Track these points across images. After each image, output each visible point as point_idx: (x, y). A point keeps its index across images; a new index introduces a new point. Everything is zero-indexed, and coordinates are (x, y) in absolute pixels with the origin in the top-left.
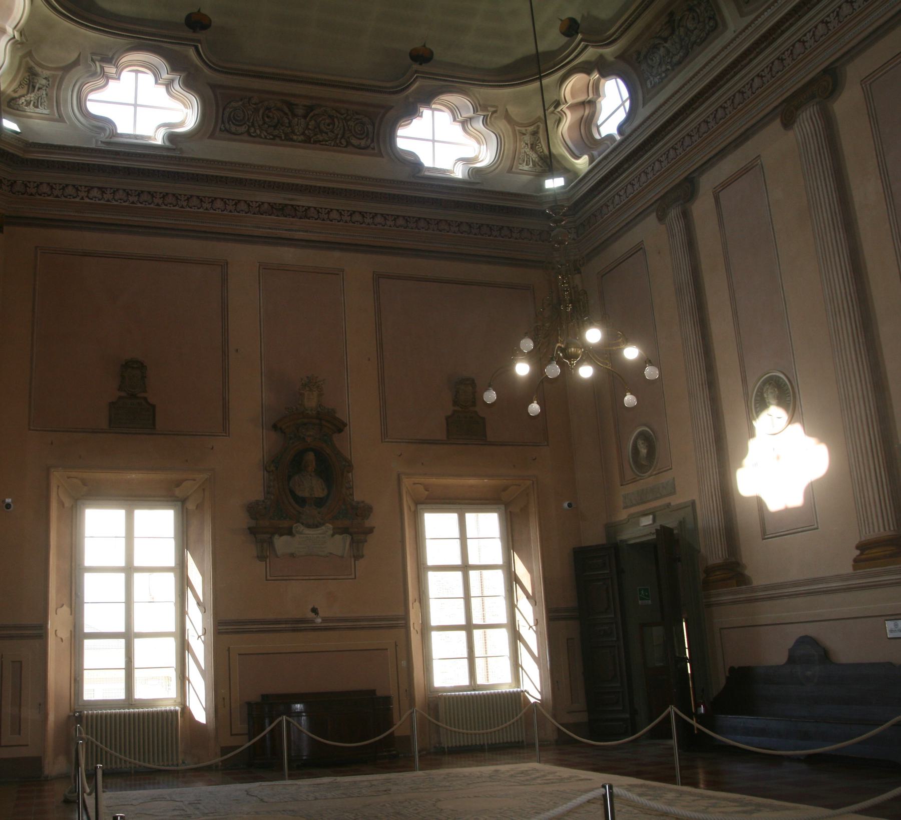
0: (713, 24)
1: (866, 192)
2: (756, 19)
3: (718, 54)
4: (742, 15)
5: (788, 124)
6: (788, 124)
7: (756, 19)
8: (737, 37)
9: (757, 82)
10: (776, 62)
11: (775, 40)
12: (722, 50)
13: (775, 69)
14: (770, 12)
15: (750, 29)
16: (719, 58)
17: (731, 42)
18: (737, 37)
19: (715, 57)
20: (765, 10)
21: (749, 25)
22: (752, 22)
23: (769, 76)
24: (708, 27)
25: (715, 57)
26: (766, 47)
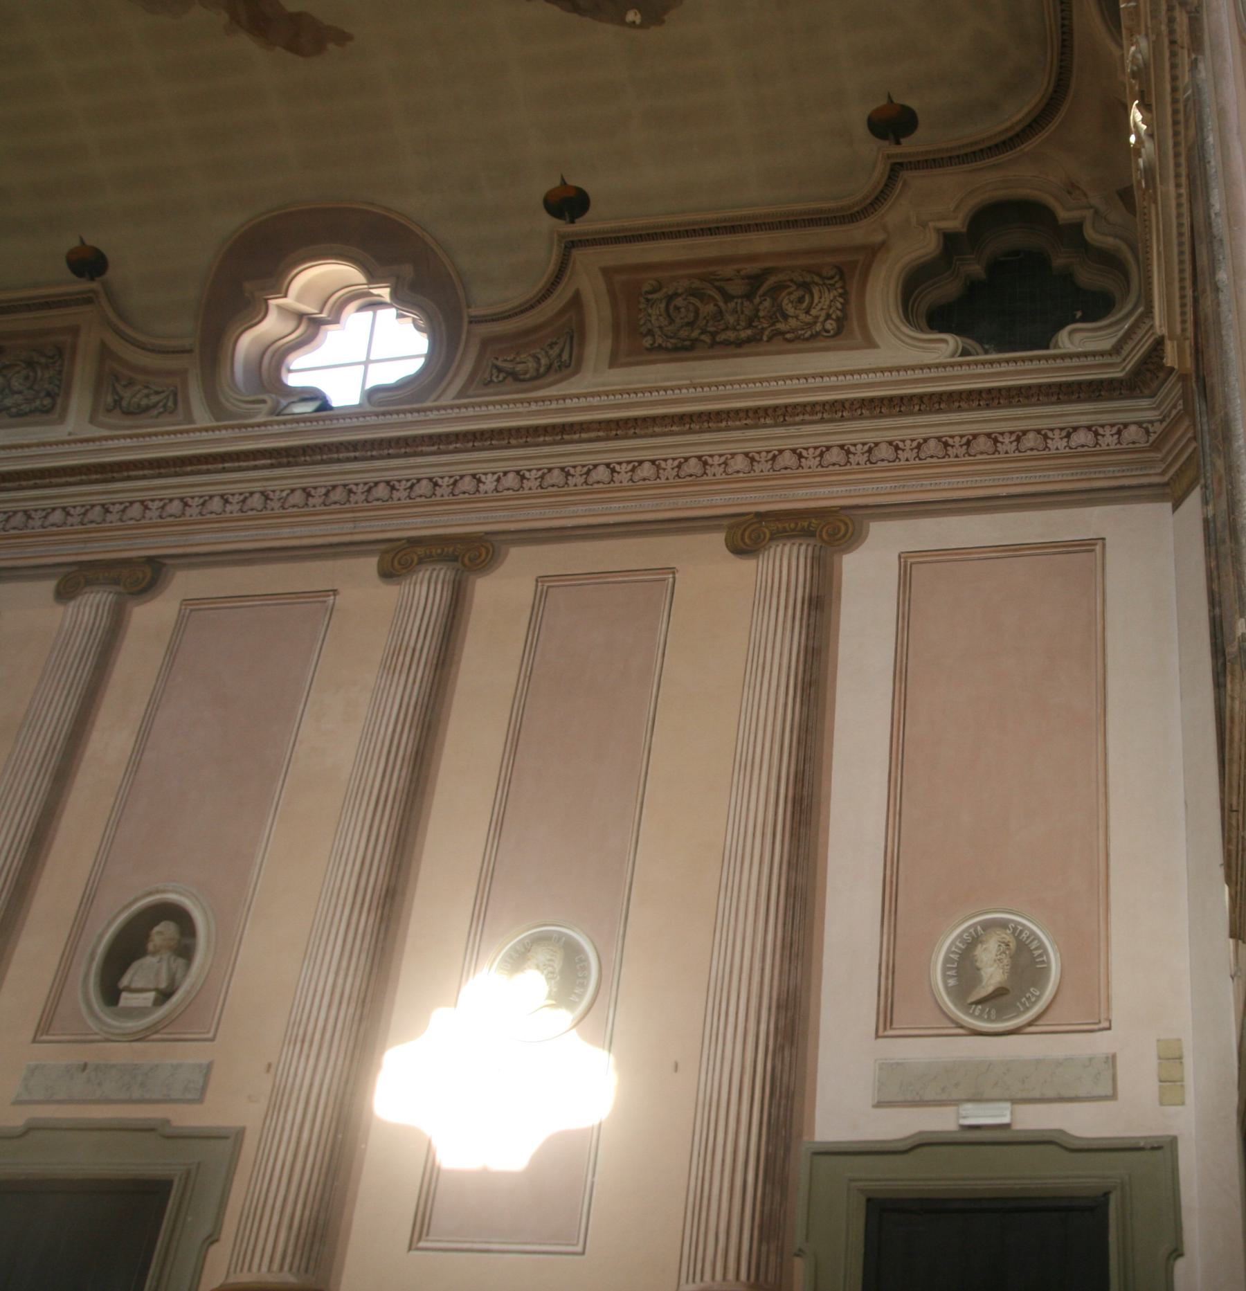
0: (49, 405)
1: (110, 741)
2: (106, 438)
3: (28, 446)
4: (93, 420)
5: (65, 593)
6: (65, 593)
7: (106, 438)
8: (69, 442)
9: (57, 516)
10: (98, 509)
11: (113, 480)
12: (38, 445)
13: (90, 516)
14: (128, 442)
15: (91, 446)
16: (27, 452)
17: (57, 443)
18: (69, 442)
19: (22, 446)
20: (124, 437)
21: (93, 440)
22: (100, 439)
23: (76, 520)
24: (38, 403)
25: (22, 446)
26: (97, 482)
